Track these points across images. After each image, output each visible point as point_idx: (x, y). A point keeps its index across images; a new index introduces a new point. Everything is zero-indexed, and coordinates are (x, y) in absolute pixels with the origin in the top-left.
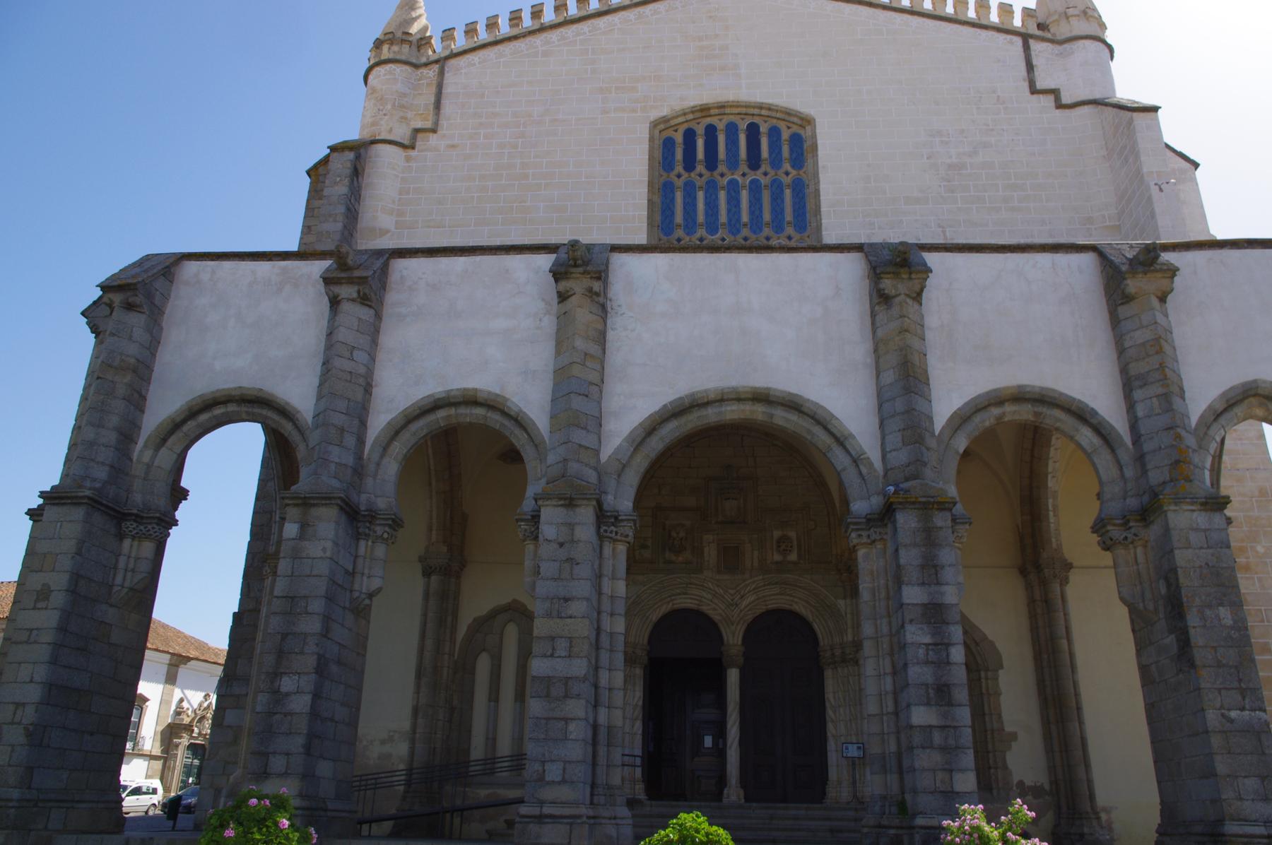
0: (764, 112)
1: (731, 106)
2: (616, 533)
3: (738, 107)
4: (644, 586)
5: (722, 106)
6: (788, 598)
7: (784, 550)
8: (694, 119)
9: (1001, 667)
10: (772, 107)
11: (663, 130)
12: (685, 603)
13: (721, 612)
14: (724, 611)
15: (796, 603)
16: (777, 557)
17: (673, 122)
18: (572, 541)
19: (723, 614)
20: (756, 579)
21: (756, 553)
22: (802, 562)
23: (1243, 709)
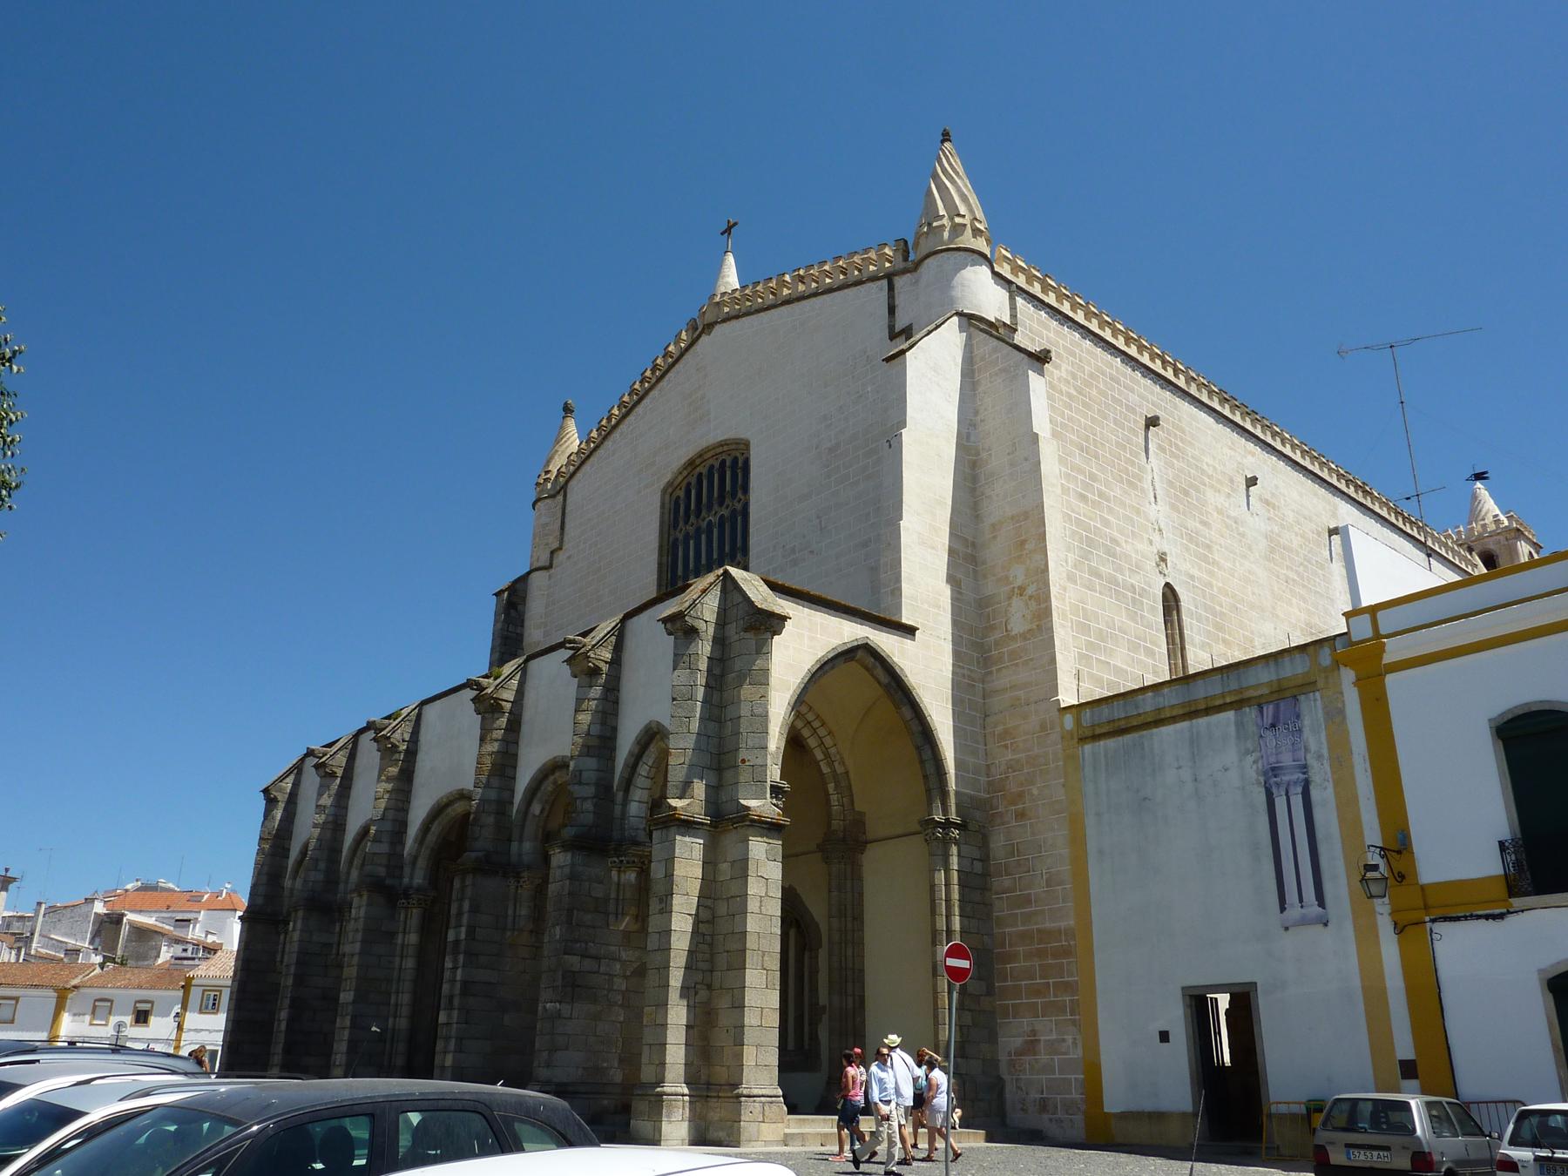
0: (725, 448)
1: (705, 453)
2: (409, 903)
3: (709, 451)
5: (700, 455)
8: (689, 474)
9: (821, 946)
10: (728, 442)
11: (673, 492)
17: (676, 483)
18: (359, 918)
23: (551, 1002)
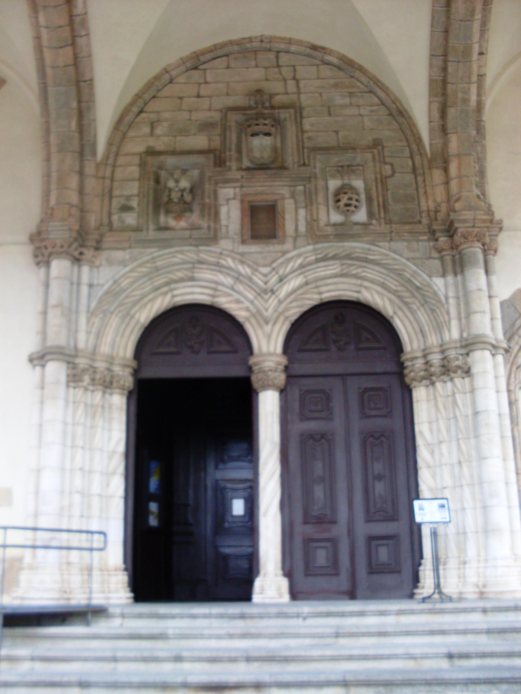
4: (125, 266)
6: (353, 281)
7: (347, 205)
12: (192, 293)
13: (247, 304)
14: (252, 302)
15: (366, 288)
16: (336, 218)
19: (251, 307)
20: (303, 250)
21: (302, 212)
22: (374, 222)
